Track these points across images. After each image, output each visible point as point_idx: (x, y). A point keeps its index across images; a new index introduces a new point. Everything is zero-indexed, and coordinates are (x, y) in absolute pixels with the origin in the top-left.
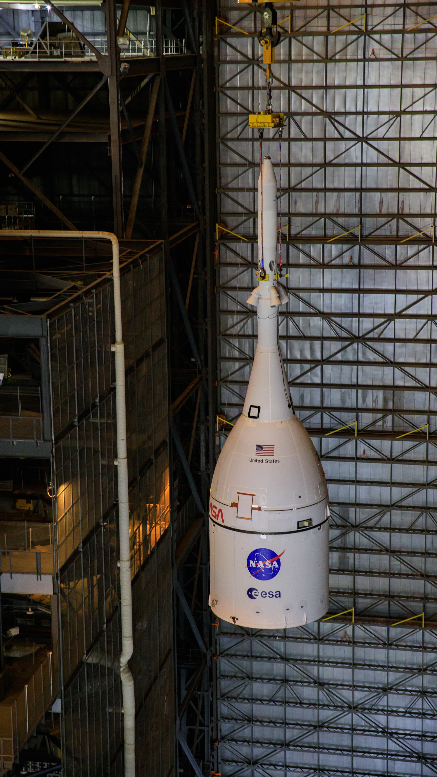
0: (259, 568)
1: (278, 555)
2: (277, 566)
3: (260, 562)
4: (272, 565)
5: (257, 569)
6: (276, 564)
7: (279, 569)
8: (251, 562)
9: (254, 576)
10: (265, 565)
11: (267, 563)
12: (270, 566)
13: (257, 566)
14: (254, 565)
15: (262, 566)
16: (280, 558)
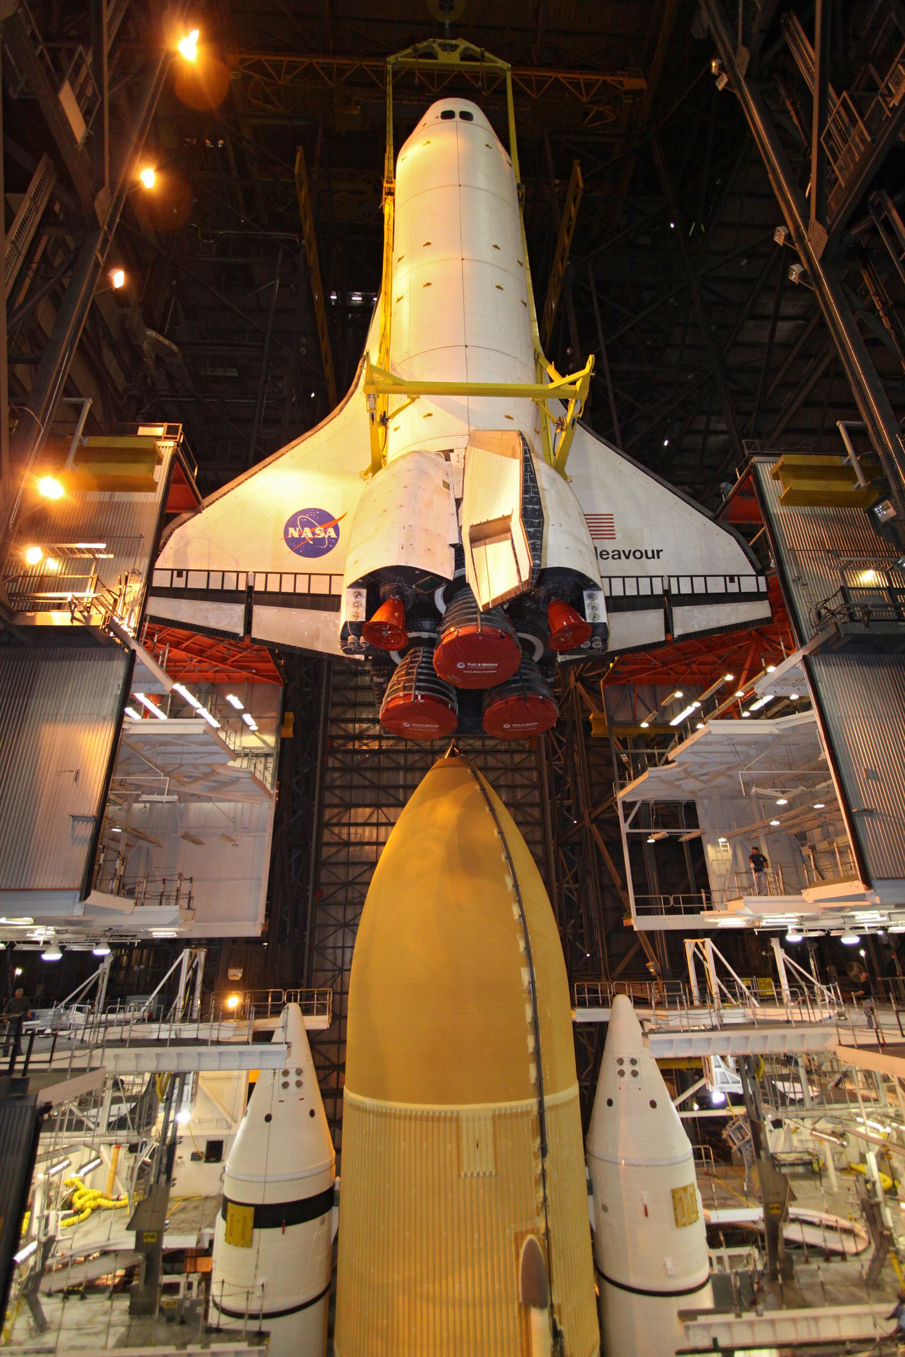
0: (304, 539)
1: (336, 517)
2: (333, 535)
3: (307, 530)
4: (325, 533)
5: (301, 539)
6: (331, 532)
7: (336, 540)
8: (291, 530)
9: (295, 551)
10: (314, 533)
11: (317, 531)
12: (322, 535)
13: (300, 535)
14: (296, 535)
15: (311, 536)
16: (339, 523)
